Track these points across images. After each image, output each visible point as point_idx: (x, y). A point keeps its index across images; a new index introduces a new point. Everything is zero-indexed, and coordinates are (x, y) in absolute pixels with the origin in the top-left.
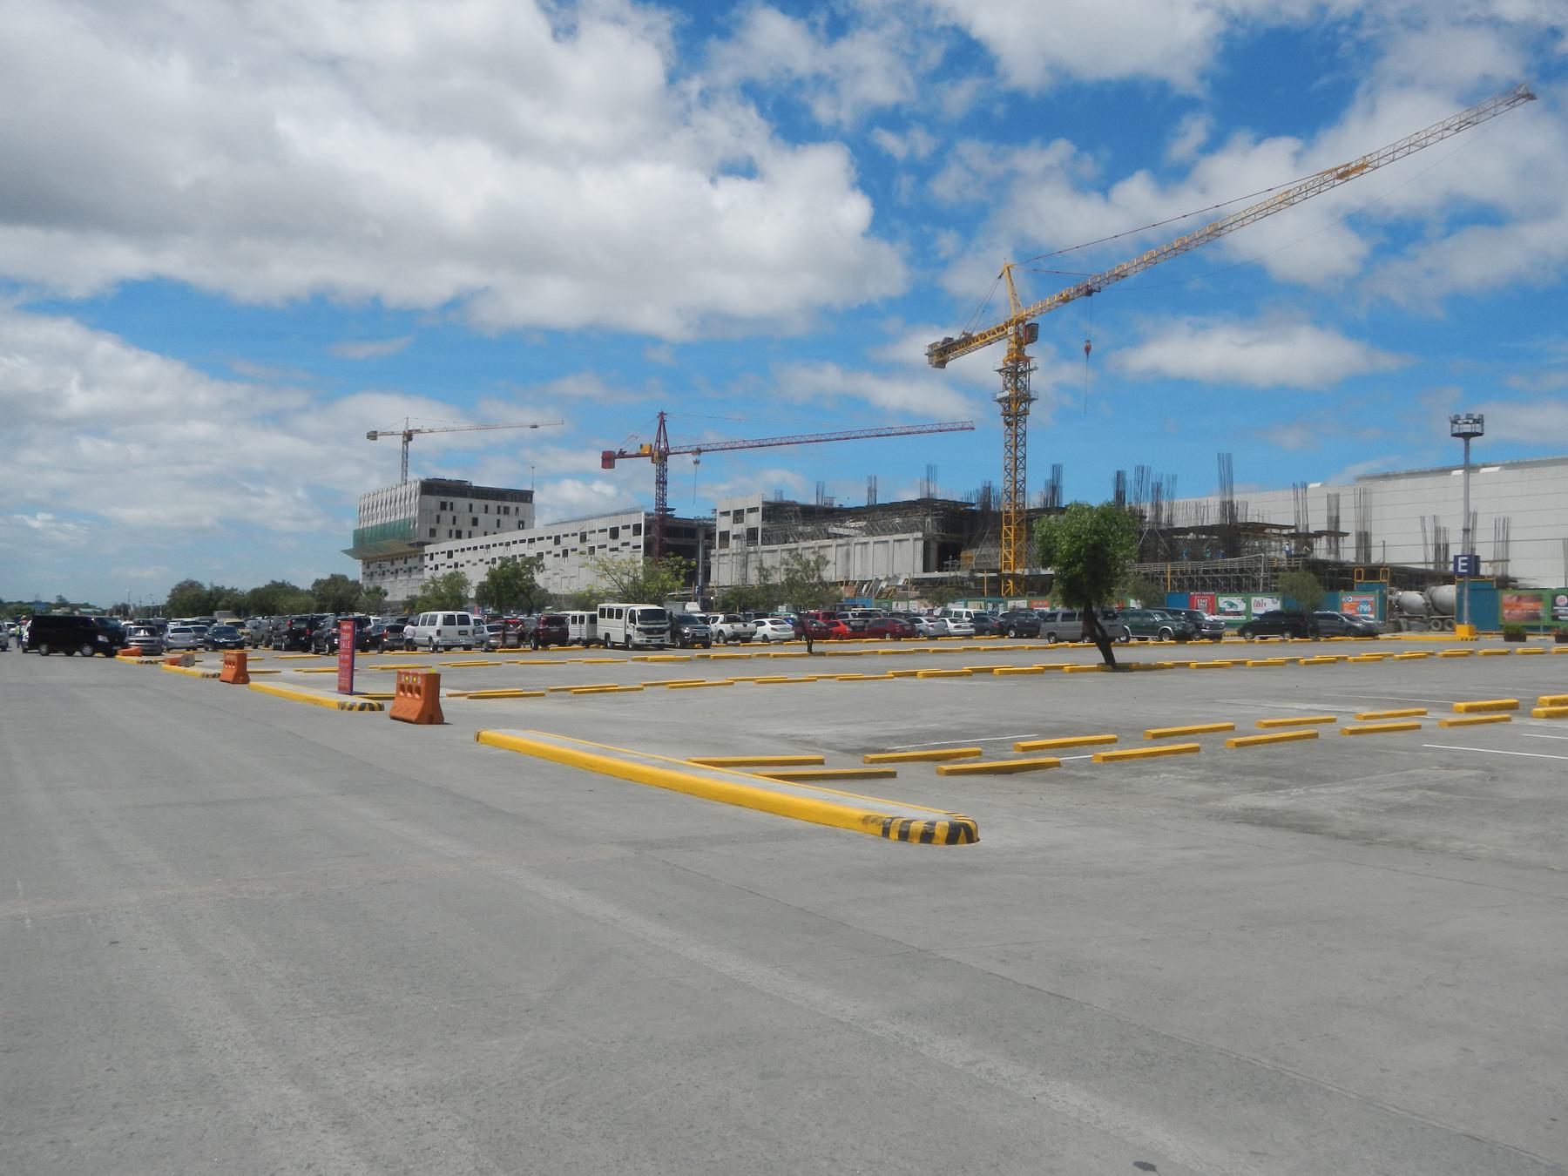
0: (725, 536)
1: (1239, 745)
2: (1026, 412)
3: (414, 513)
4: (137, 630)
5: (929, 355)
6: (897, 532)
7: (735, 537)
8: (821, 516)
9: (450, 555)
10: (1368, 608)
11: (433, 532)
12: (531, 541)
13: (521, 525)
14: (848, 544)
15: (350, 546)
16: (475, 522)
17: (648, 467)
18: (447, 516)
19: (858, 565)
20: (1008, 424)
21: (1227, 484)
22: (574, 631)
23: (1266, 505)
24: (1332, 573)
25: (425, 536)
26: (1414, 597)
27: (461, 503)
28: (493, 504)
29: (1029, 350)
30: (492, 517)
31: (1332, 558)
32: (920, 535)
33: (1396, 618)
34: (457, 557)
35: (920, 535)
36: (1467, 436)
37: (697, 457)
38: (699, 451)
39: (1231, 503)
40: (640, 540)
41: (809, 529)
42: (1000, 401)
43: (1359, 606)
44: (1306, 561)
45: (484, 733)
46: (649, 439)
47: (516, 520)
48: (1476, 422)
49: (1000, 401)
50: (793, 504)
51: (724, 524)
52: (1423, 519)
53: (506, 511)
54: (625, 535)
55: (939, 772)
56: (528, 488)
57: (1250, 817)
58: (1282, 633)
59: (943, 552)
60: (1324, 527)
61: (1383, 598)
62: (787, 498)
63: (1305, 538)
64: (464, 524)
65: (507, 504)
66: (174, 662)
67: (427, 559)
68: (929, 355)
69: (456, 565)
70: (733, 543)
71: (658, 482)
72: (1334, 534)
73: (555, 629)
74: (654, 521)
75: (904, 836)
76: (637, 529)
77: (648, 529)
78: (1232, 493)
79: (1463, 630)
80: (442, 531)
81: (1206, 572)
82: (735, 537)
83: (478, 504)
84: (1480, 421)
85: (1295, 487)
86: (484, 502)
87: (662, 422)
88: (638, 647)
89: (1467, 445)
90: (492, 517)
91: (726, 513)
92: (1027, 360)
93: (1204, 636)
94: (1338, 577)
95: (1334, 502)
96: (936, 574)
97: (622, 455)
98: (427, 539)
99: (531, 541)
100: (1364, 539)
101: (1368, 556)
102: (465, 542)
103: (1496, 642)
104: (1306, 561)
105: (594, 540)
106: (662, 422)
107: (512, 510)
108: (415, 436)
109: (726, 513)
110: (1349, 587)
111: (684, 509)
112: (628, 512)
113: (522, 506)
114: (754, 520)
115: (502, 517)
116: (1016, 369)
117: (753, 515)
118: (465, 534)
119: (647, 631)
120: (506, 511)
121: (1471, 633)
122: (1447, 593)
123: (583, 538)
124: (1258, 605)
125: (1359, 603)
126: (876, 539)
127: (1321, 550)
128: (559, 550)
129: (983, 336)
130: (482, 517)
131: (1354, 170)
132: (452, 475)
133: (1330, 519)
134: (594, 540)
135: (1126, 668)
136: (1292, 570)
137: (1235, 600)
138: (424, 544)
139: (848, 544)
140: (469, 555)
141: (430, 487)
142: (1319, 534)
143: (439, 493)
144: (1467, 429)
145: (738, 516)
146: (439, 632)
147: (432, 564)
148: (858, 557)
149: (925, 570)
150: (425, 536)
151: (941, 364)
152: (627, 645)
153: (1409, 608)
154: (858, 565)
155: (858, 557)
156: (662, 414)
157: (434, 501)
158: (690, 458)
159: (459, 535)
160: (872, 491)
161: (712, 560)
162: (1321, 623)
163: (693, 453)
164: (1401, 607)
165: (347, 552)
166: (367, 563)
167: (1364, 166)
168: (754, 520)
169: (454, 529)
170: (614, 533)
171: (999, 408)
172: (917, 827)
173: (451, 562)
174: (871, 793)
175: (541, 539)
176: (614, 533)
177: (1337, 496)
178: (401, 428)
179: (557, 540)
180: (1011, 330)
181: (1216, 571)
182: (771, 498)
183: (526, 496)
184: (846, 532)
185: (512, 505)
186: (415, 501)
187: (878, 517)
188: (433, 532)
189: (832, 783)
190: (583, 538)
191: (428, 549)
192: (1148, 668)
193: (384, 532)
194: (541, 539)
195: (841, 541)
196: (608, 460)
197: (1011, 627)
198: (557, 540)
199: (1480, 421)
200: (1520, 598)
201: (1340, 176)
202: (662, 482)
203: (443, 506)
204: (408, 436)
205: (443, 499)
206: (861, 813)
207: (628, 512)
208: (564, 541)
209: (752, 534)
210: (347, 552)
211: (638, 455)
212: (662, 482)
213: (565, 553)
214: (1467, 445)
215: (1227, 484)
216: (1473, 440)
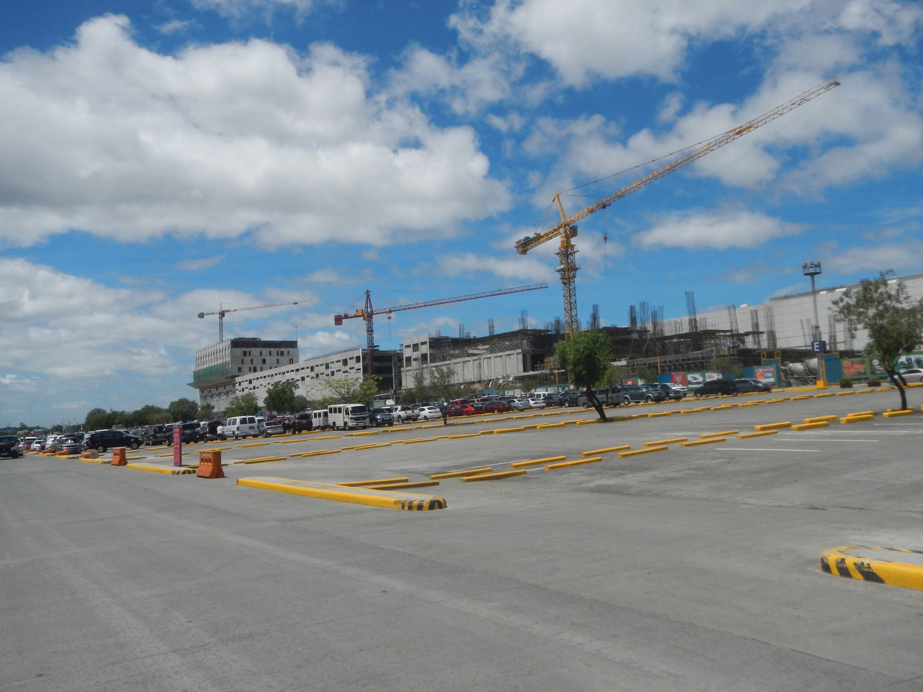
0: (409, 359)
1: (623, 456)
2: (574, 276)
3: (228, 359)
4: (67, 440)
5: (517, 247)
6: (507, 350)
7: (415, 360)
8: (462, 345)
9: (250, 382)
10: (770, 375)
11: (240, 369)
12: (297, 370)
13: (291, 361)
14: (479, 359)
15: (192, 380)
16: (264, 361)
17: (361, 323)
18: (247, 359)
19: (486, 370)
20: (565, 284)
21: (692, 309)
22: (316, 422)
23: (715, 319)
24: (754, 356)
26: (798, 366)
27: (255, 351)
28: (274, 350)
29: (573, 241)
30: (274, 358)
31: (756, 347)
32: (520, 351)
33: (786, 379)
34: (255, 383)
35: (520, 351)
36: (812, 275)
37: (390, 315)
38: (391, 311)
39: (696, 321)
40: (360, 365)
41: (457, 352)
42: (559, 271)
43: (765, 375)
44: (738, 350)
45: (240, 480)
46: (361, 305)
47: (288, 359)
48: (816, 266)
49: (559, 271)
50: (446, 338)
51: (408, 353)
52: (801, 321)
53: (282, 354)
54: (351, 363)
55: (462, 481)
56: (294, 340)
57: (600, 490)
58: (716, 393)
59: (534, 360)
60: (750, 330)
61: (778, 370)
62: (443, 334)
63: (740, 337)
64: (258, 365)
65: (282, 349)
66: (87, 457)
67: (237, 385)
68: (517, 247)
69: (254, 388)
70: (414, 363)
71: (368, 331)
72: (756, 333)
73: (304, 421)
74: (367, 354)
75: (410, 508)
76: (358, 359)
77: (364, 358)
78: (695, 314)
79: (820, 384)
80: (245, 368)
81: (683, 360)
82: (415, 360)
83: (265, 351)
84: (818, 266)
85: (729, 308)
86: (268, 350)
87: (368, 296)
88: (352, 429)
89: (813, 280)
90: (274, 358)
91: (408, 346)
92: (573, 246)
93: (671, 398)
94: (751, 358)
95: (754, 314)
96: (531, 373)
97: (346, 317)
99: (297, 370)
100: (772, 336)
101: (775, 345)
102: (258, 374)
103: (836, 389)
104: (738, 350)
105: (334, 367)
106: (368, 296)
107: (286, 353)
108: (226, 314)
109: (408, 346)
110: (759, 364)
111: (384, 345)
112: (352, 350)
113: (291, 350)
114: (425, 349)
115: (280, 357)
116: (567, 252)
117: (424, 346)
118: (258, 369)
119: (356, 419)
120: (282, 354)
121: (825, 385)
122: (814, 362)
123: (327, 367)
124: (710, 377)
125: (765, 372)
126: (495, 355)
127: (750, 343)
128: (313, 374)
129: (546, 235)
130: (268, 359)
131: (745, 130)
132: (249, 335)
133: (753, 325)
134: (334, 367)
135: (611, 420)
136: (731, 355)
137: (696, 375)
138: (234, 377)
139: (479, 359)
140: (261, 381)
141: (236, 343)
142: (747, 334)
144: (812, 271)
145: (416, 347)
146: (238, 428)
147: (240, 388)
148: (486, 366)
149: (525, 370)
151: (524, 252)
152: (346, 427)
153: (798, 373)
154: (486, 370)
155: (486, 366)
156: (368, 291)
157: (239, 351)
158: (387, 316)
159: (255, 370)
160: (491, 327)
161: (403, 374)
162: (739, 386)
163: (387, 312)
164: (793, 373)
165: (190, 385)
166: (202, 390)
167: (749, 127)
168: (425, 349)
169: (252, 366)
170: (345, 362)
171: (558, 275)
172: (416, 503)
173: (251, 386)
174: (419, 492)
175: (303, 369)
176: (345, 362)
177: (756, 311)
178: (218, 310)
179: (312, 369)
180: (562, 230)
181: (689, 359)
182: (434, 335)
183: (293, 344)
184: (478, 352)
185: (285, 350)
186: (228, 352)
187: (496, 342)
188: (240, 369)
189: (414, 489)
190: (327, 367)
191: (238, 379)
192: (623, 419)
193: (210, 371)
194: (303, 369)
195: (475, 358)
196: (338, 320)
197: (566, 401)
198: (312, 369)
199: (818, 266)
200: (853, 363)
201: (738, 133)
202: (370, 331)
203: (245, 353)
204: (222, 314)
205: (245, 349)
206: (394, 500)
207: (352, 350)
208: (316, 369)
209: (424, 357)
210: (190, 385)
211: (355, 316)
212: (370, 331)
213: (317, 376)
214: (813, 280)
215: (692, 309)
216: (816, 277)
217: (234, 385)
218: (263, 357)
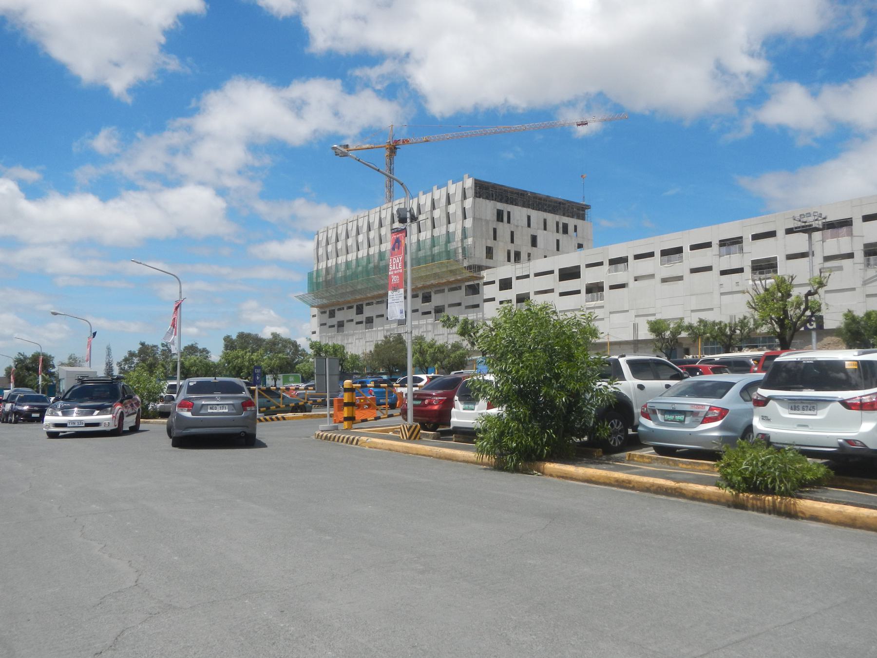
11: (489, 252)
16: (534, 241)
18: (504, 229)
25: (479, 256)
27: (519, 213)
28: (552, 219)
53: (565, 230)
67: (488, 291)
83: (537, 216)
98: (485, 262)
107: (571, 229)
113: (579, 223)
115: (560, 236)
118: (524, 256)
130: (541, 235)
138: (480, 268)
143: (488, 197)
150: (479, 256)
157: (489, 207)
166: (328, 310)
169: (513, 248)
185: (571, 222)
188: (489, 252)
191: (486, 275)
203: (500, 216)
204: (393, 150)
205: (500, 206)
217: (474, 290)
218: (532, 231)
